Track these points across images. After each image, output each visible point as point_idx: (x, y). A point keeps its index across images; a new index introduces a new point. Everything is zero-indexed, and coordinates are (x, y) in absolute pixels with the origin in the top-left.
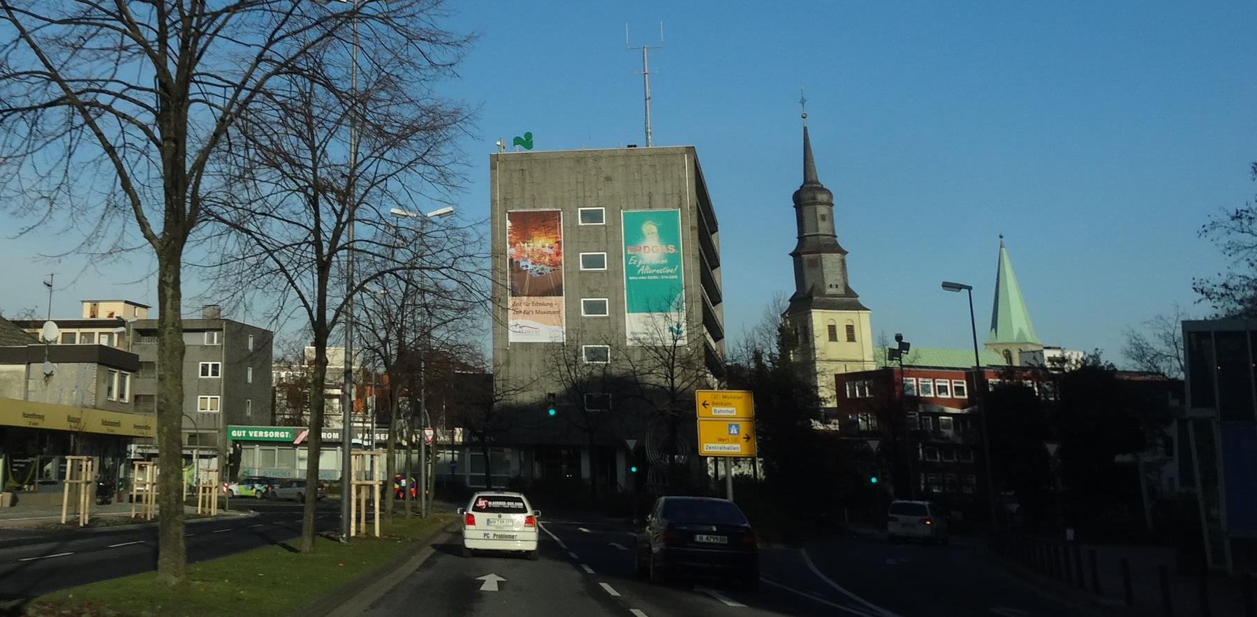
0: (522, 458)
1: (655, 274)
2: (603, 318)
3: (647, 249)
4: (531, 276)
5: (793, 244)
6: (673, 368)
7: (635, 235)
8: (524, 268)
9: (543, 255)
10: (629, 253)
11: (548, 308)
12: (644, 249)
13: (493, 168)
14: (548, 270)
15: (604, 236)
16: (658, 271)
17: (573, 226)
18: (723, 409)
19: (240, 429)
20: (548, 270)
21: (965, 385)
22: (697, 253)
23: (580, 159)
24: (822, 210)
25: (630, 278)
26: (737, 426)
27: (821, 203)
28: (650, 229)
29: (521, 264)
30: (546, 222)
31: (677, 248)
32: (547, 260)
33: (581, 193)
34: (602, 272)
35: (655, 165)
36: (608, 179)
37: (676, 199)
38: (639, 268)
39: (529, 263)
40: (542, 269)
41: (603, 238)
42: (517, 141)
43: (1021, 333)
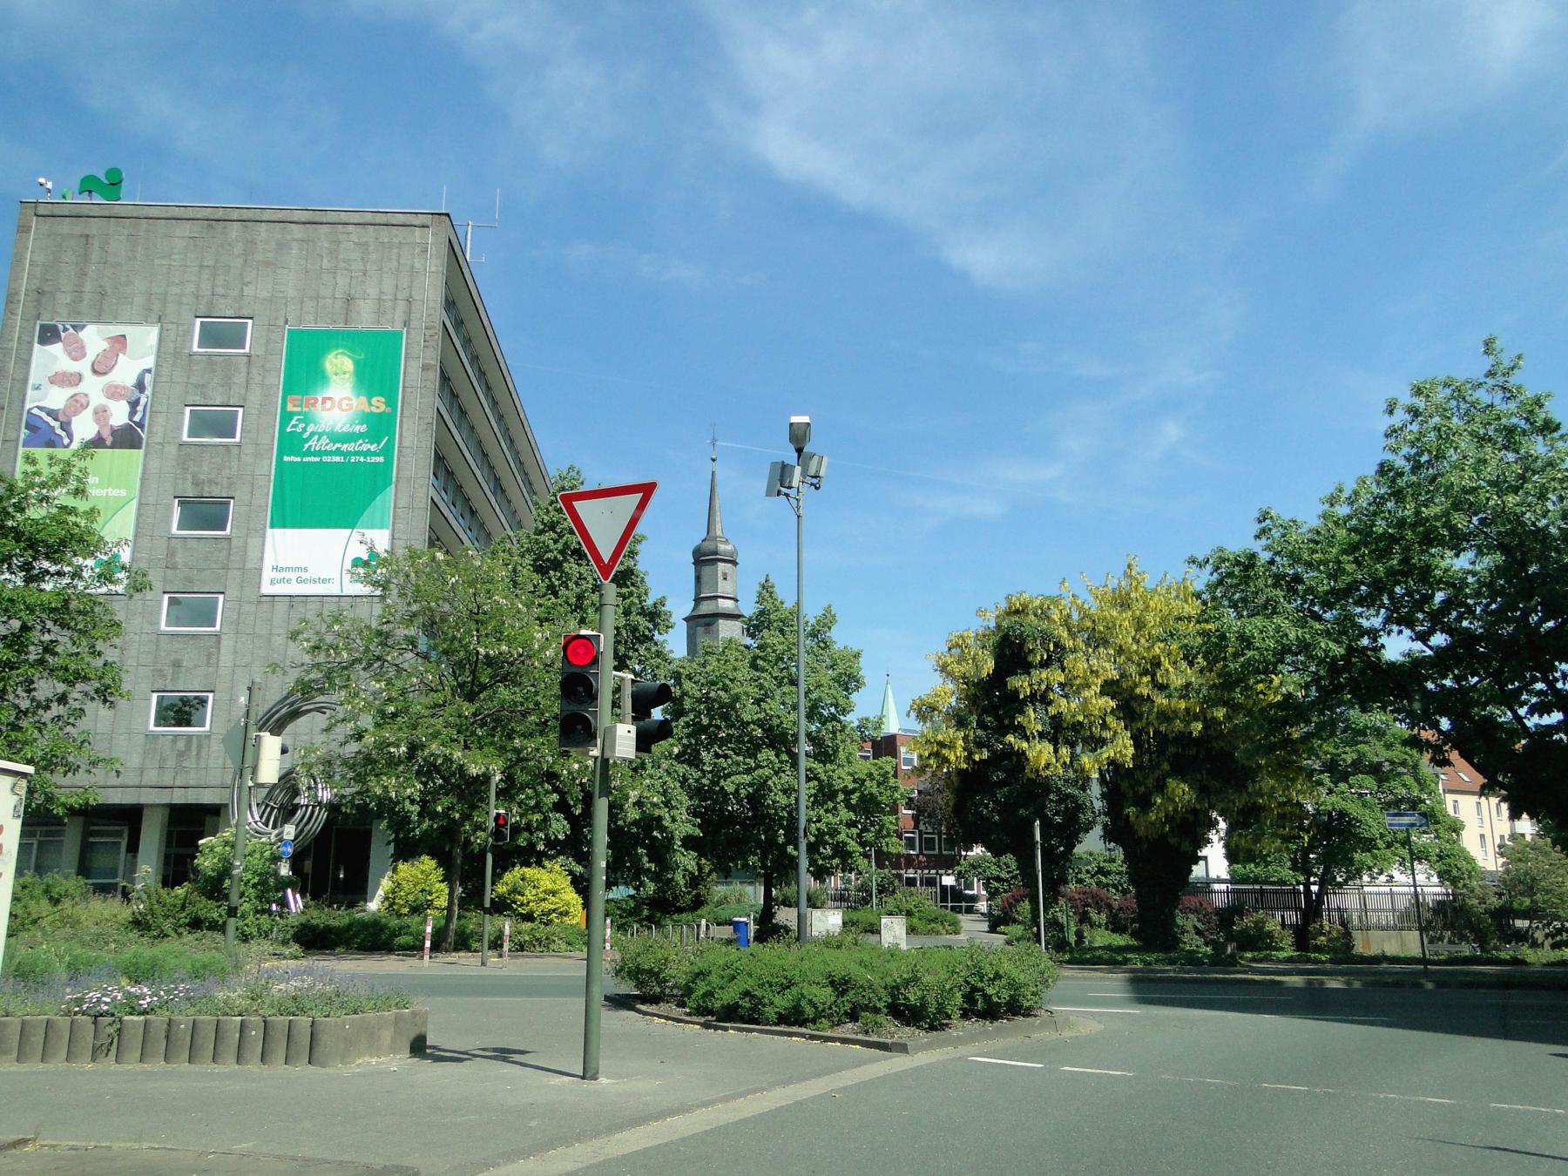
1: (338, 452)
3: (328, 402)
10: (290, 408)
12: (323, 403)
15: (244, 375)
22: (431, 416)
25: (286, 459)
31: (391, 403)
33: (206, 288)
34: (226, 446)
37: (402, 306)
38: (307, 440)
41: (240, 379)
42: (89, 184)
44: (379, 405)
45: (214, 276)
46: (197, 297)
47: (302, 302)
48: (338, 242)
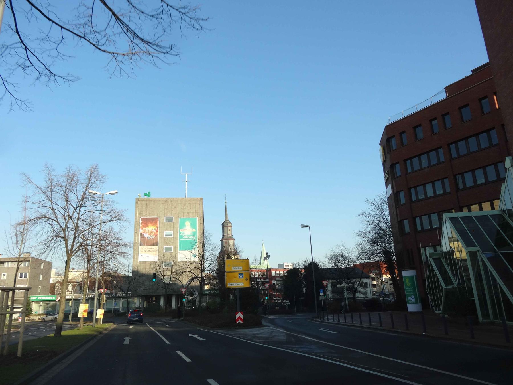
1: (188, 238)
4: (147, 239)
7: (183, 225)
8: (145, 236)
9: (152, 232)
10: (180, 231)
11: (153, 250)
13: (137, 203)
14: (153, 237)
16: (189, 237)
17: (163, 223)
18: (237, 267)
19: (36, 297)
20: (153, 237)
23: (166, 201)
24: (229, 228)
25: (181, 239)
26: (242, 274)
27: (229, 226)
28: (188, 224)
29: (145, 235)
30: (153, 221)
31: (196, 230)
32: (153, 233)
33: (166, 212)
34: (171, 238)
35: (190, 204)
37: (196, 214)
38: (183, 236)
39: (147, 235)
40: (151, 237)
41: (172, 227)
42: (145, 194)
44: (194, 230)
45: (167, 209)
46: (165, 213)
47: (181, 214)
48: (186, 203)
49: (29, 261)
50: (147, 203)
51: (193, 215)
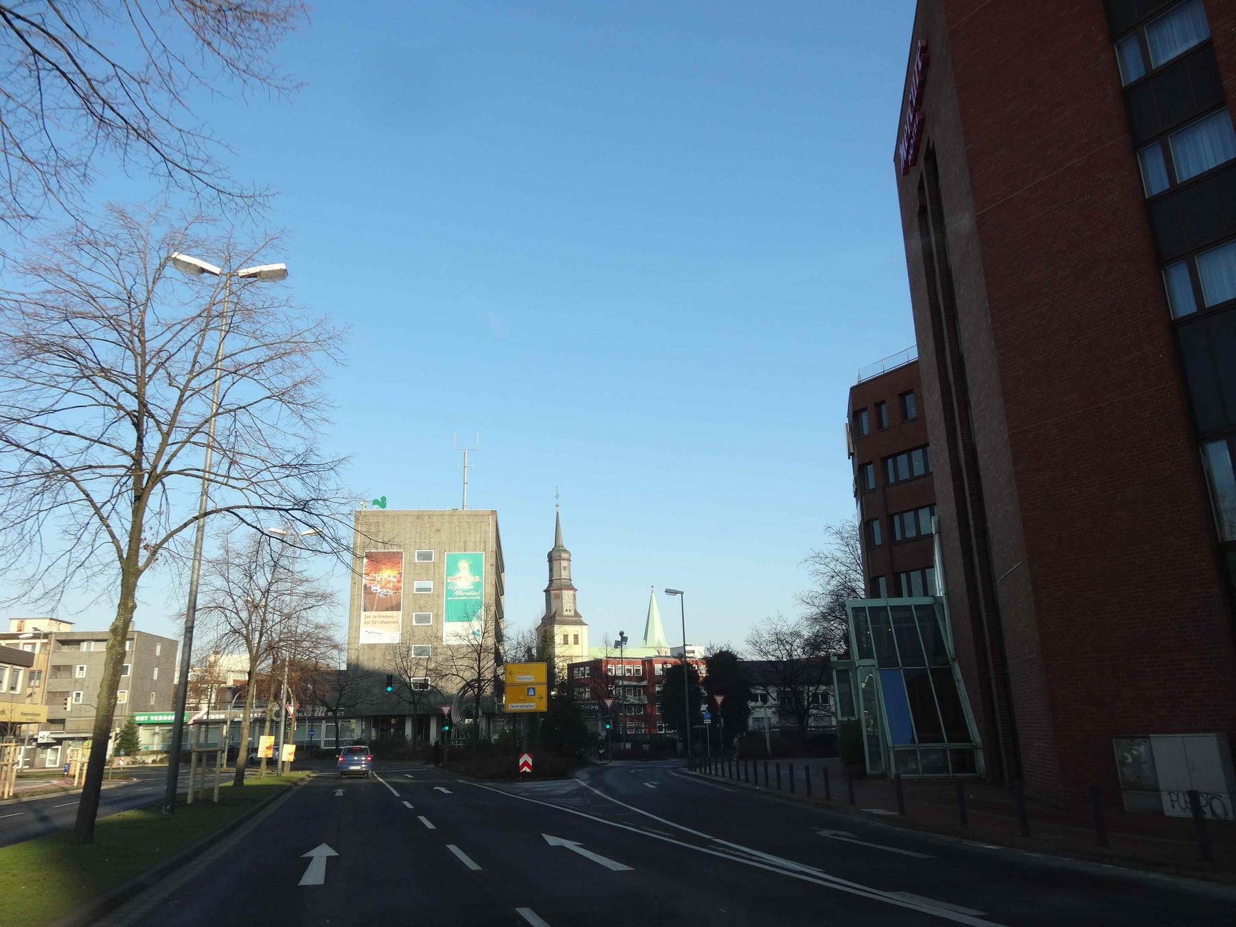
0: (364, 726)
1: (465, 595)
2: (428, 626)
4: (379, 597)
5: (546, 584)
6: (480, 653)
7: (453, 569)
8: (374, 591)
9: (389, 582)
11: (390, 619)
14: (391, 592)
17: (411, 563)
20: (391, 592)
21: (641, 668)
23: (419, 516)
24: (564, 563)
25: (449, 598)
27: (564, 559)
28: (464, 565)
29: (373, 588)
30: (393, 559)
32: (392, 584)
33: (418, 540)
34: (429, 595)
35: (470, 522)
36: (438, 530)
37: (482, 545)
39: (378, 588)
40: (387, 592)
42: (375, 502)
43: (659, 642)
44: (477, 579)
45: (421, 535)
46: (416, 543)
49: (133, 639)
50: (380, 521)
51: (475, 546)
